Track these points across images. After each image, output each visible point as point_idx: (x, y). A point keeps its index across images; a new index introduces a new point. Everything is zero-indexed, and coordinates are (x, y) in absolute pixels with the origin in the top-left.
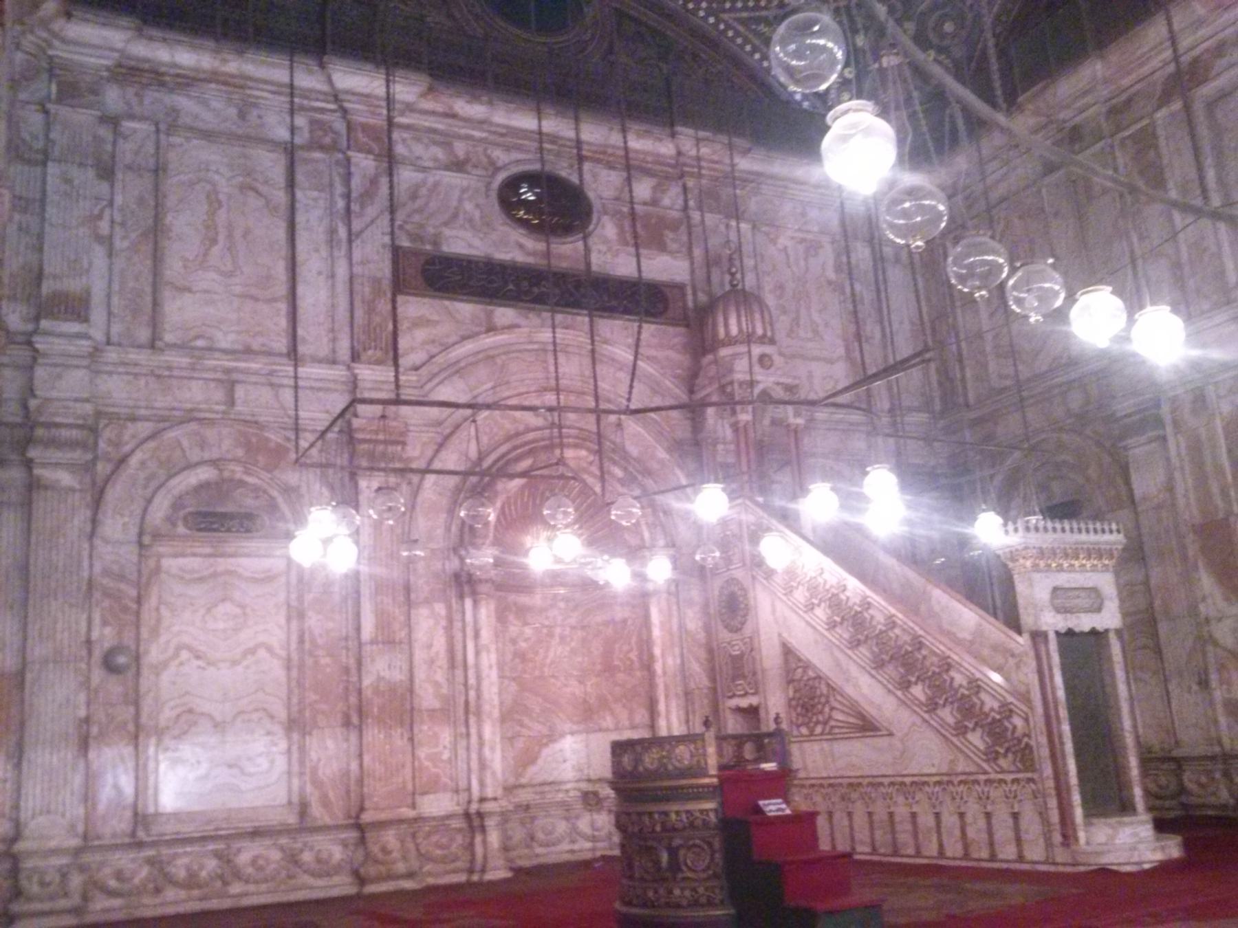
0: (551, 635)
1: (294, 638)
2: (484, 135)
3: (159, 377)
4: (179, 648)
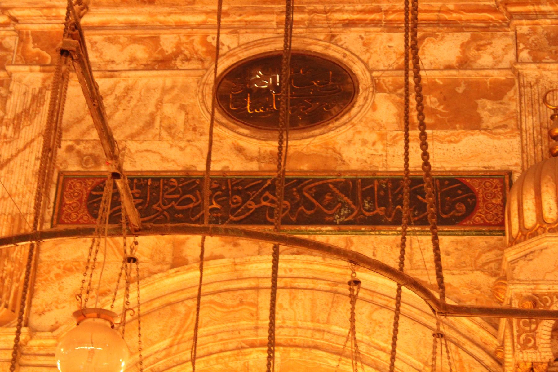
2: (200, 18)
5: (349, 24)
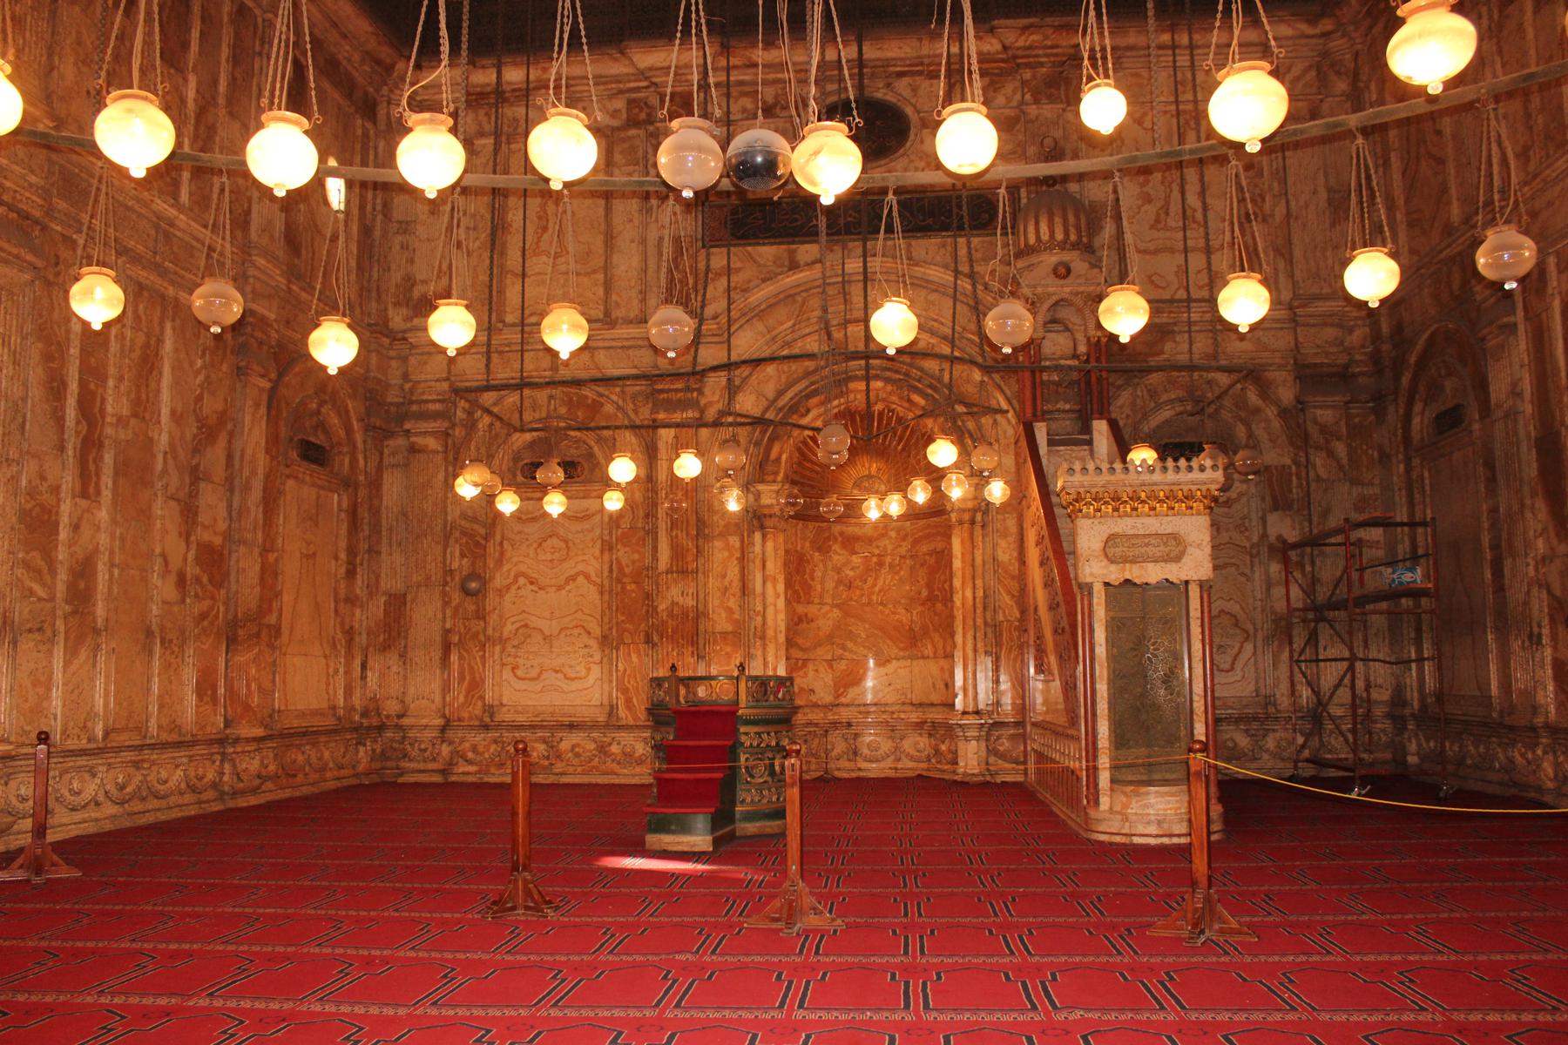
0: (881, 564)
1: (606, 567)
3: (502, 352)
4: (517, 576)
5: (900, 75)
